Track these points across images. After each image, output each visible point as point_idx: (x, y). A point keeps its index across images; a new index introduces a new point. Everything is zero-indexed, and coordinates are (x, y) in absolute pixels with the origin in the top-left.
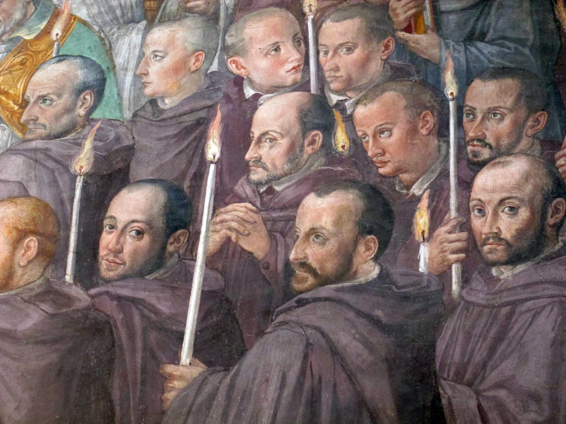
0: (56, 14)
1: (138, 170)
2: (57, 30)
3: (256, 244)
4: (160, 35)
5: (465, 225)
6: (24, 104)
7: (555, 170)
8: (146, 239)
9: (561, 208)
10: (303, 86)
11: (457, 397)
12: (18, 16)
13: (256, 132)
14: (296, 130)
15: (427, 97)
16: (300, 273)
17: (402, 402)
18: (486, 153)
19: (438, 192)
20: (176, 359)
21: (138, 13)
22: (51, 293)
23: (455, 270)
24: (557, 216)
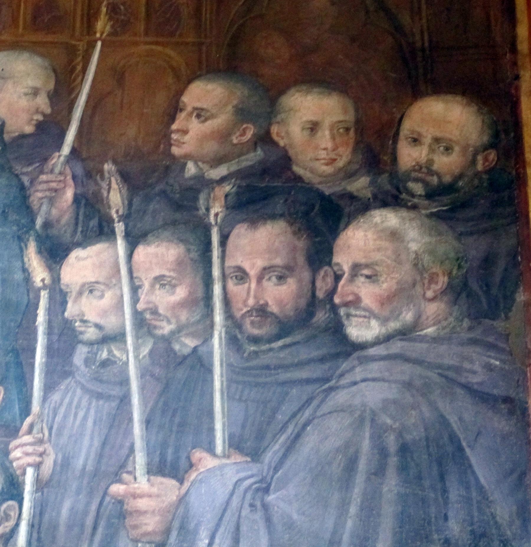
7: (8, 464)
9: (12, 514)
24: (7, 524)
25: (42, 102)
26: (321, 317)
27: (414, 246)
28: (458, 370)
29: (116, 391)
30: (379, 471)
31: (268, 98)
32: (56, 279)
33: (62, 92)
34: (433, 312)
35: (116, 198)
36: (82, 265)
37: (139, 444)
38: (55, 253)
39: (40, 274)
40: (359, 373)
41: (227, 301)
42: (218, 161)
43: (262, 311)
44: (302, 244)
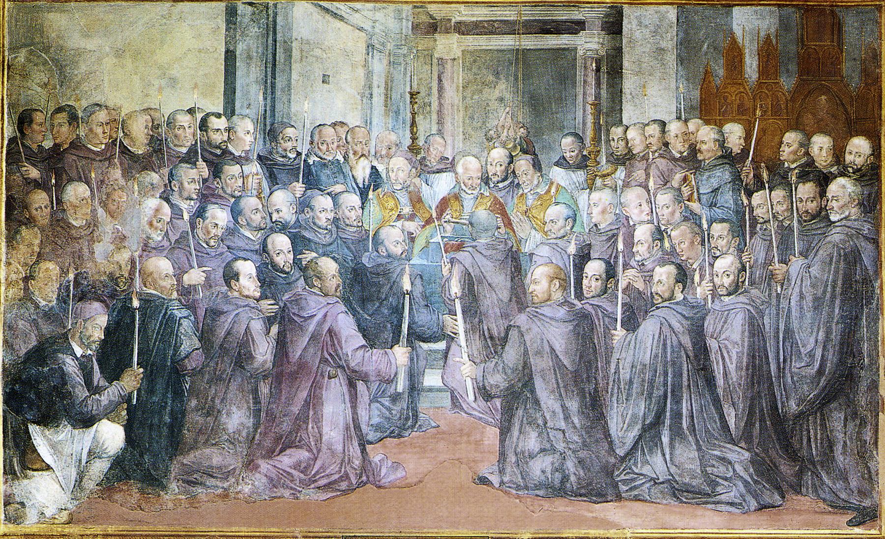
0: (552, 183)
1: (593, 255)
2: (553, 190)
3: (640, 285)
4: (595, 195)
5: (712, 281)
6: (545, 223)
8: (600, 282)
10: (651, 222)
11: (712, 344)
12: (536, 182)
13: (636, 241)
14: (651, 240)
15: (696, 229)
16: (656, 297)
17: (694, 344)
18: (718, 253)
19: (702, 268)
20: (615, 329)
21: (586, 186)
22: (566, 302)
23: (710, 296)
25: (742, 141)
26: (823, 213)
27: (849, 190)
28: (860, 230)
29: (769, 238)
30: (838, 261)
31: (809, 136)
32: (750, 203)
33: (748, 138)
34: (854, 212)
35: (765, 175)
36: (757, 198)
37: (776, 255)
38: (749, 194)
39: (746, 202)
40: (834, 231)
41: (797, 209)
42: (793, 162)
43: (807, 212)
44: (818, 190)
